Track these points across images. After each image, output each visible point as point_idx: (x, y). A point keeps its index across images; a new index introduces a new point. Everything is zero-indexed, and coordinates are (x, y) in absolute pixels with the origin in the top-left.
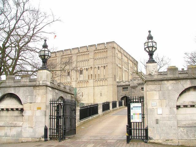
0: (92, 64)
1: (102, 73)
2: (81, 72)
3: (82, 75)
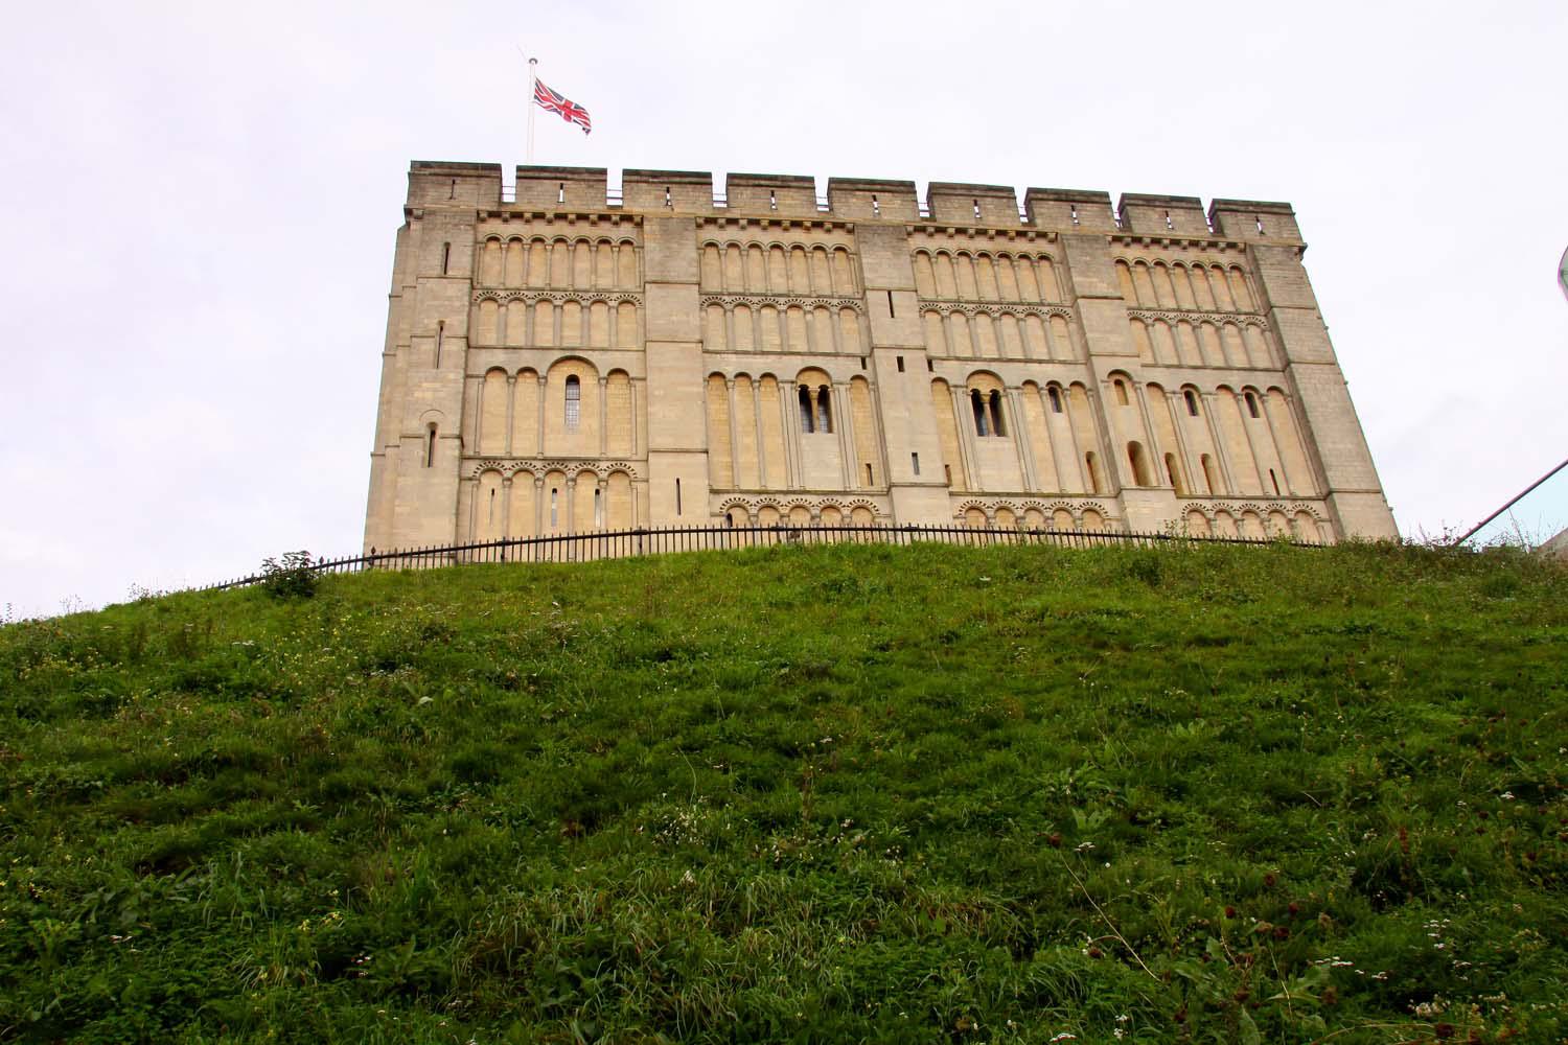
1: (1236, 448)
2: (988, 409)
3: (991, 442)
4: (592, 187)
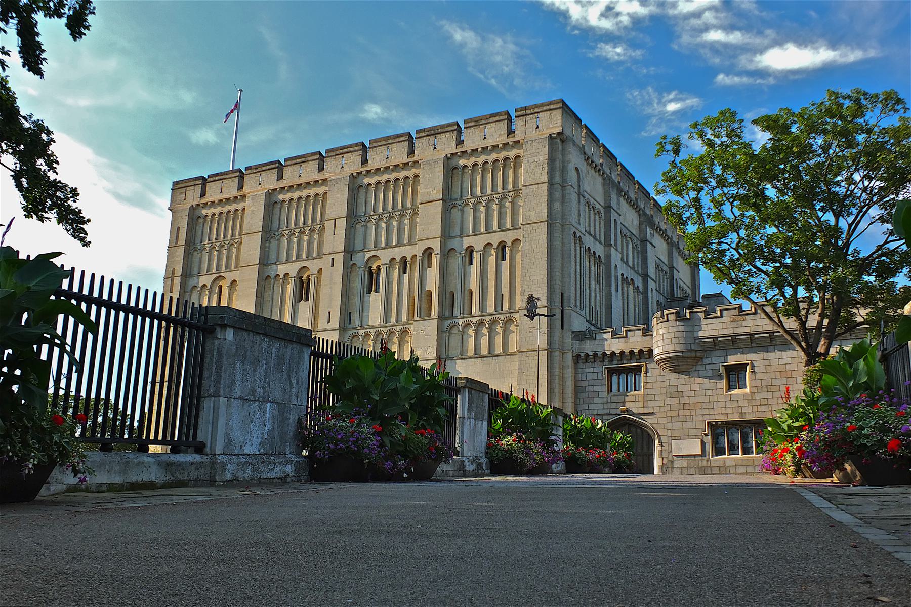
0: (436, 229)
4: (233, 181)
